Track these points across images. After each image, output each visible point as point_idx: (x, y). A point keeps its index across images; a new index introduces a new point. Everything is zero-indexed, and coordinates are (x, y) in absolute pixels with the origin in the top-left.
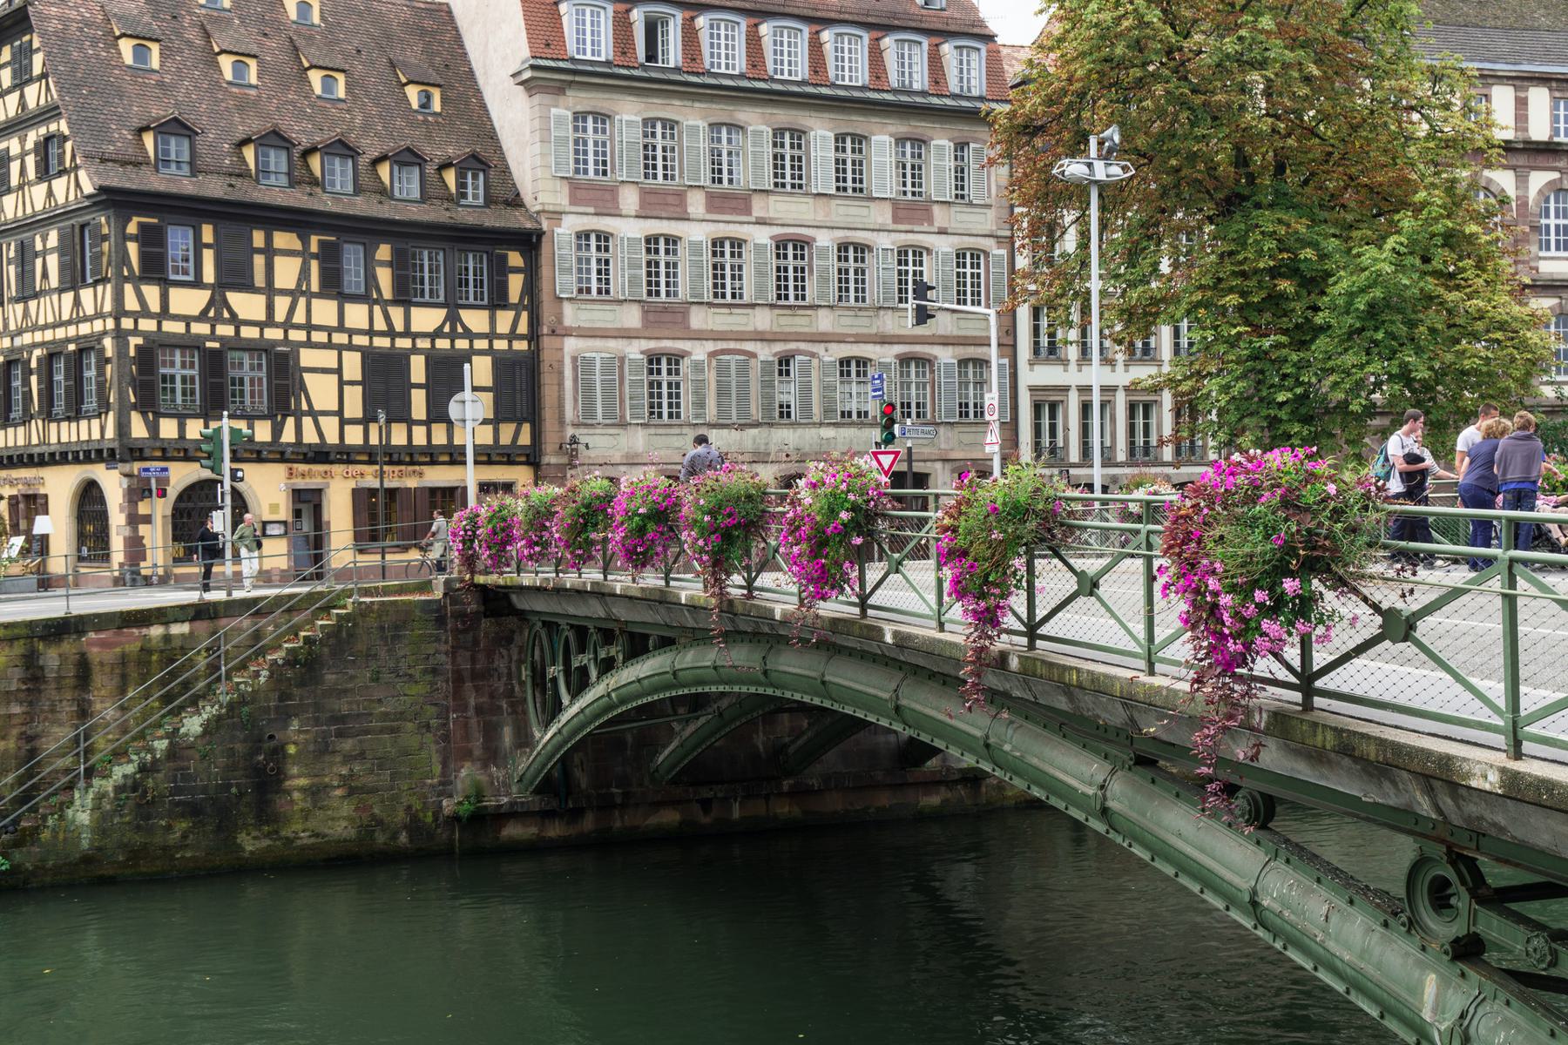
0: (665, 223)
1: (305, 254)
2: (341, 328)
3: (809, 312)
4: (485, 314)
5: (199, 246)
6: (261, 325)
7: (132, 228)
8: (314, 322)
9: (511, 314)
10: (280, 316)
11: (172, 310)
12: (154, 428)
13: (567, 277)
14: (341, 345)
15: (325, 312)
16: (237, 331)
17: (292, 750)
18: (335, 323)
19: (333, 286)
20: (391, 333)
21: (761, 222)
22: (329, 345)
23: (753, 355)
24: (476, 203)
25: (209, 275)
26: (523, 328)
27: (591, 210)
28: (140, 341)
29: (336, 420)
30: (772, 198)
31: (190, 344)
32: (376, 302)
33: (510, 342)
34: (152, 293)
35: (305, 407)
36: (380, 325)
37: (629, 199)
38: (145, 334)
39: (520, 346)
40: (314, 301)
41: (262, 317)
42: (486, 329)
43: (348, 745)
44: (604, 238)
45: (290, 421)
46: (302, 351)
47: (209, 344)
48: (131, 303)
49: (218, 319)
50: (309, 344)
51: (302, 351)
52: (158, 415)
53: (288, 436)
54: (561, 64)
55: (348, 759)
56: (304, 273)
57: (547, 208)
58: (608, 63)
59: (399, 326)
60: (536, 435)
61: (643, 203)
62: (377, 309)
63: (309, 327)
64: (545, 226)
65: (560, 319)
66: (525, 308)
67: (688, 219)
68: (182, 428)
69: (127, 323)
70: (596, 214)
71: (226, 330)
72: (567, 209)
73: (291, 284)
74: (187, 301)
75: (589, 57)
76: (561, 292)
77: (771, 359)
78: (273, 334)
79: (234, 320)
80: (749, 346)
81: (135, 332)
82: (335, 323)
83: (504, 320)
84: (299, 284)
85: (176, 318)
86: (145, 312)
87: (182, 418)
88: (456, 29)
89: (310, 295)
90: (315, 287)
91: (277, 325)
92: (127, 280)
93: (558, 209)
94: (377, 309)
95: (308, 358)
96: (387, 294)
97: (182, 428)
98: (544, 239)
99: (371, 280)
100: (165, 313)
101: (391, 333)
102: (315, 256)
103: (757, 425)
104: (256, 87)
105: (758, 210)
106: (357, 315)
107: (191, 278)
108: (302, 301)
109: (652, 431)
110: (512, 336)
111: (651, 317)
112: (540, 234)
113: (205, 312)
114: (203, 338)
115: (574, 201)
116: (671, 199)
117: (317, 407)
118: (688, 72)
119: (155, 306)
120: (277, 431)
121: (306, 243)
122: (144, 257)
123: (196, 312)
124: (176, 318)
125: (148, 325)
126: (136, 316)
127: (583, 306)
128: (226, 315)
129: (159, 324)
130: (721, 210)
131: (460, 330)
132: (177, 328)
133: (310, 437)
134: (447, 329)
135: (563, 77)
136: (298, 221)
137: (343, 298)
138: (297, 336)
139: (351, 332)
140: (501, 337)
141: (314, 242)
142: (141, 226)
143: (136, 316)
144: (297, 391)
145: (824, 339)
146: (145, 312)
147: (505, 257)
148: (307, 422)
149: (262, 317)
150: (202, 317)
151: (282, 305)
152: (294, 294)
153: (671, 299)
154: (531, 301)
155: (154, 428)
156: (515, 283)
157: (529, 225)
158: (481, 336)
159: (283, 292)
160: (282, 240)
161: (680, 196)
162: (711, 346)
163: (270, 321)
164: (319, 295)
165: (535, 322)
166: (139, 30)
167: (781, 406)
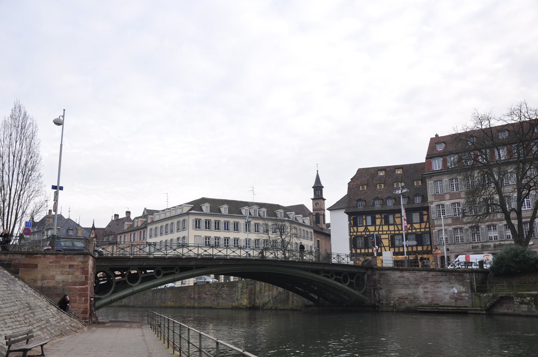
0: (456, 200)
1: (381, 218)
2: (389, 230)
4: (419, 224)
6: (374, 232)
8: (384, 230)
9: (425, 224)
10: (377, 230)
11: (359, 231)
12: (356, 251)
13: (434, 215)
15: (385, 228)
17: (290, 295)
18: (387, 230)
19: (387, 223)
20: (399, 230)
22: (387, 234)
24: (419, 202)
25: (364, 224)
26: (427, 226)
27: (439, 200)
28: (353, 237)
29: (388, 247)
31: (362, 236)
32: (395, 225)
33: (425, 229)
34: (355, 228)
35: (382, 245)
36: (396, 229)
37: (447, 197)
38: (354, 235)
39: (428, 230)
40: (383, 226)
41: (374, 230)
42: (419, 227)
44: (443, 205)
46: (382, 235)
48: (352, 231)
49: (366, 231)
50: (383, 234)
51: (382, 235)
54: (430, 173)
56: (381, 221)
57: (429, 201)
58: (441, 170)
61: (450, 197)
63: (383, 231)
64: (429, 205)
65: (434, 223)
66: (428, 222)
69: (352, 234)
71: (368, 233)
73: (379, 224)
75: (438, 169)
76: (433, 218)
79: (369, 231)
82: (387, 230)
83: (423, 225)
84: (380, 224)
85: (359, 232)
86: (354, 232)
87: (361, 249)
89: (382, 225)
90: (383, 224)
91: (377, 231)
92: (351, 227)
93: (432, 201)
94: (396, 226)
95: (382, 237)
99: (394, 221)
100: (357, 232)
102: (383, 218)
106: (392, 228)
108: (381, 226)
109: (456, 245)
110: (425, 228)
114: (364, 235)
115: (435, 199)
116: (457, 195)
117: (385, 245)
119: (356, 231)
121: (381, 216)
122: (353, 223)
124: (359, 232)
125: (355, 234)
126: (353, 233)
131: (413, 228)
132: (360, 234)
134: (410, 228)
135: (431, 175)
136: (380, 212)
138: (380, 233)
139: (391, 231)
140: (423, 228)
141: (383, 215)
142: (353, 217)
143: (353, 233)
146: (354, 232)
147: (423, 212)
149: (374, 230)
150: (364, 231)
151: (377, 228)
152: (379, 225)
155: (356, 251)
156: (425, 218)
157: (426, 205)
158: (418, 229)
159: (378, 225)
160: (377, 216)
163: (375, 231)
164: (385, 225)
166: (362, 184)
167: (490, 237)
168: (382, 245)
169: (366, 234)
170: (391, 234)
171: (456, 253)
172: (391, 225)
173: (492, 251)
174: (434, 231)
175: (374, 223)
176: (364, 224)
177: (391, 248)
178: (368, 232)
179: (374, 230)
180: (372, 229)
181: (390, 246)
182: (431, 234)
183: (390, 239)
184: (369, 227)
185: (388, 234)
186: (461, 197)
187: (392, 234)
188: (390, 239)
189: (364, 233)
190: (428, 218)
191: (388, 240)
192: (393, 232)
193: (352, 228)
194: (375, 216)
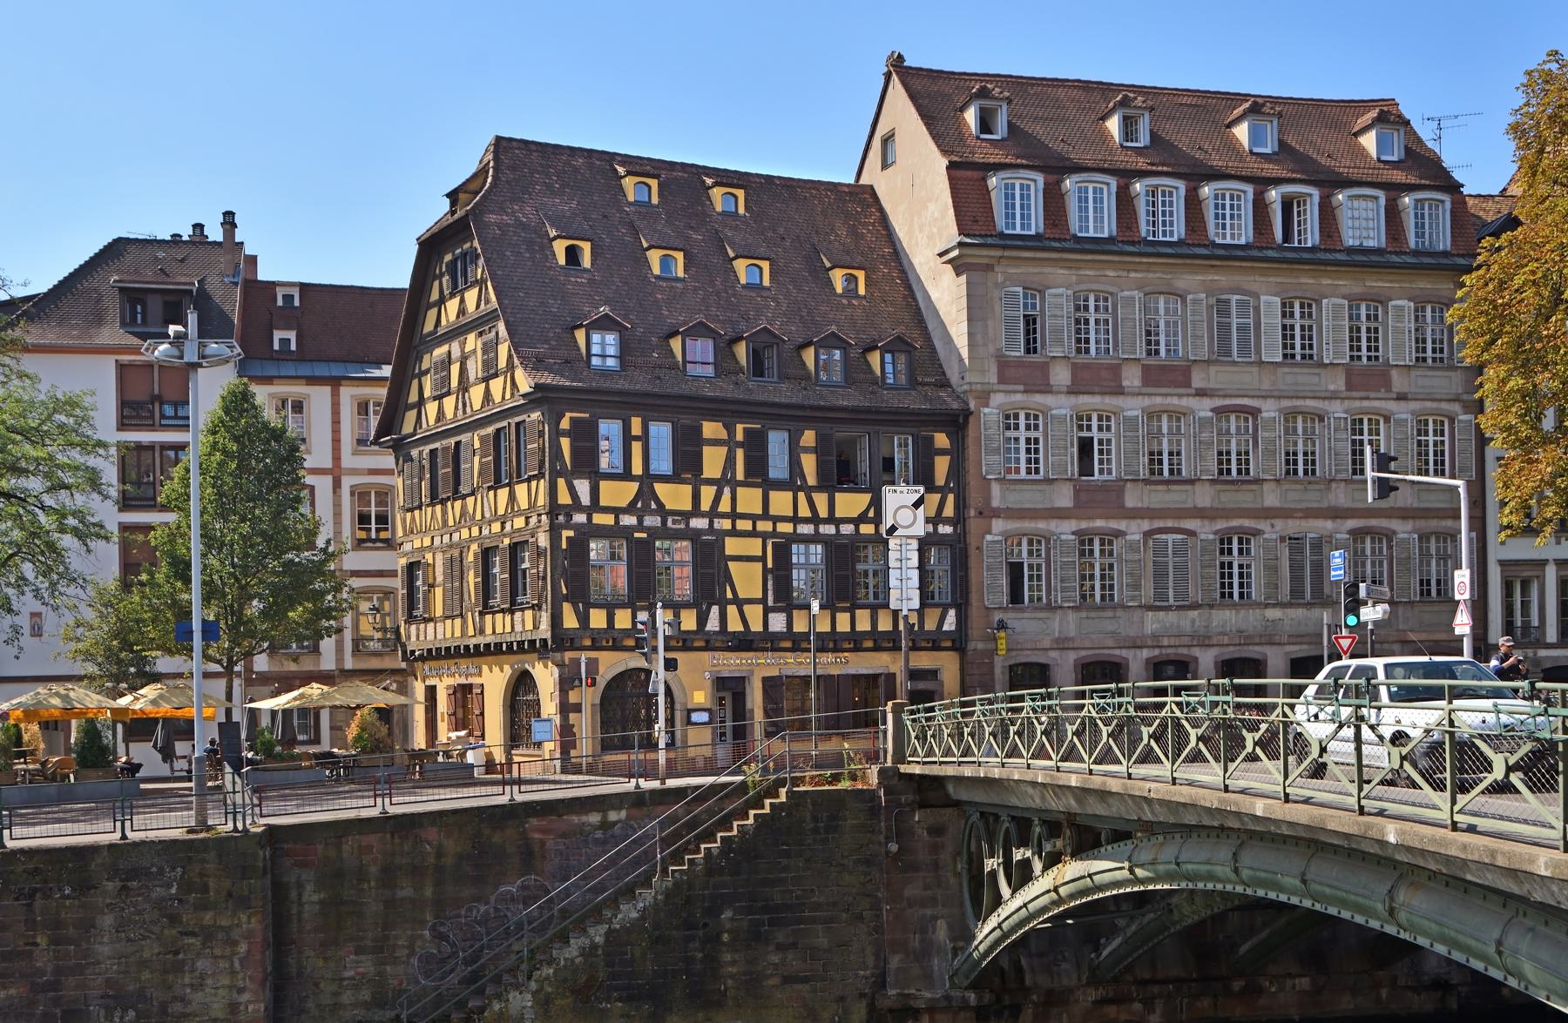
1: (730, 443)
3: (1253, 487)
5: (628, 438)
7: (565, 424)
8: (739, 510)
10: (705, 505)
11: (603, 503)
12: (584, 619)
14: (765, 532)
15: (750, 500)
16: (664, 522)
17: (725, 937)
19: (757, 472)
20: (815, 519)
21: (1201, 393)
22: (753, 533)
23: (1192, 533)
25: (637, 469)
26: (949, 511)
27: (1021, 388)
28: (571, 533)
29: (760, 607)
30: (1213, 369)
32: (800, 489)
35: (729, 595)
36: (804, 511)
38: (577, 527)
39: (945, 529)
41: (688, 507)
43: (781, 936)
45: (715, 610)
46: (727, 540)
47: (637, 535)
48: (564, 498)
49: (646, 510)
50: (734, 533)
51: (727, 540)
52: (589, 605)
53: (713, 624)
54: (989, 241)
55: (780, 948)
56: (730, 462)
59: (823, 512)
60: (962, 620)
62: (801, 495)
63: (734, 515)
66: (951, 491)
67: (1123, 394)
68: (611, 619)
70: (1025, 392)
71: (652, 521)
72: (995, 387)
74: (617, 493)
75: (1018, 231)
76: (987, 473)
77: (1211, 537)
78: (699, 523)
79: (662, 510)
80: (1189, 524)
81: (568, 526)
84: (724, 473)
87: (611, 609)
88: (881, 210)
89: (735, 485)
90: (740, 476)
91: (703, 515)
94: (801, 495)
95: (732, 546)
96: (811, 480)
97: (611, 619)
98: (972, 420)
100: (595, 507)
101: (815, 519)
102: (741, 445)
103: (1195, 606)
104: (683, 280)
105: (1198, 381)
106: (781, 502)
107: (620, 471)
108: (727, 490)
111: (1083, 496)
112: (967, 414)
113: (633, 503)
114: (629, 530)
115: (1002, 379)
117: (741, 596)
118: (1122, 242)
119: (585, 500)
120: (702, 620)
123: (624, 504)
125: (580, 518)
127: (1012, 487)
128: (654, 506)
129: (590, 518)
130: (1158, 384)
132: (606, 520)
133: (735, 625)
134: (871, 514)
137: (769, 485)
139: (776, 520)
141: (740, 428)
144: (722, 580)
145: (1269, 514)
146: (576, 505)
148: (732, 610)
149: (688, 507)
150: (630, 509)
151: (708, 493)
152: (719, 483)
153: (1105, 477)
154: (958, 484)
155: (584, 619)
156: (942, 465)
157: (955, 406)
159: (710, 482)
160: (710, 429)
161: (1115, 370)
162: (1146, 525)
163: (696, 511)
165: (960, 506)
168: (729, 595)
169: (640, 526)
170: (774, 534)
171: (1083, 653)
172: (780, 485)
173: (1232, 648)
174: (989, 537)
175: (687, 465)
176: (637, 469)
177: (775, 610)
178: (653, 513)
179: (687, 506)
180: (675, 496)
181: (770, 603)
182: (973, 552)
183: (770, 565)
184: (660, 488)
185: (765, 536)
186: (1121, 386)
187: (783, 535)
188: (770, 565)
189: (629, 520)
190: (956, 471)
191: (759, 566)
192: (784, 528)
193: (561, 482)
194: (699, 429)
